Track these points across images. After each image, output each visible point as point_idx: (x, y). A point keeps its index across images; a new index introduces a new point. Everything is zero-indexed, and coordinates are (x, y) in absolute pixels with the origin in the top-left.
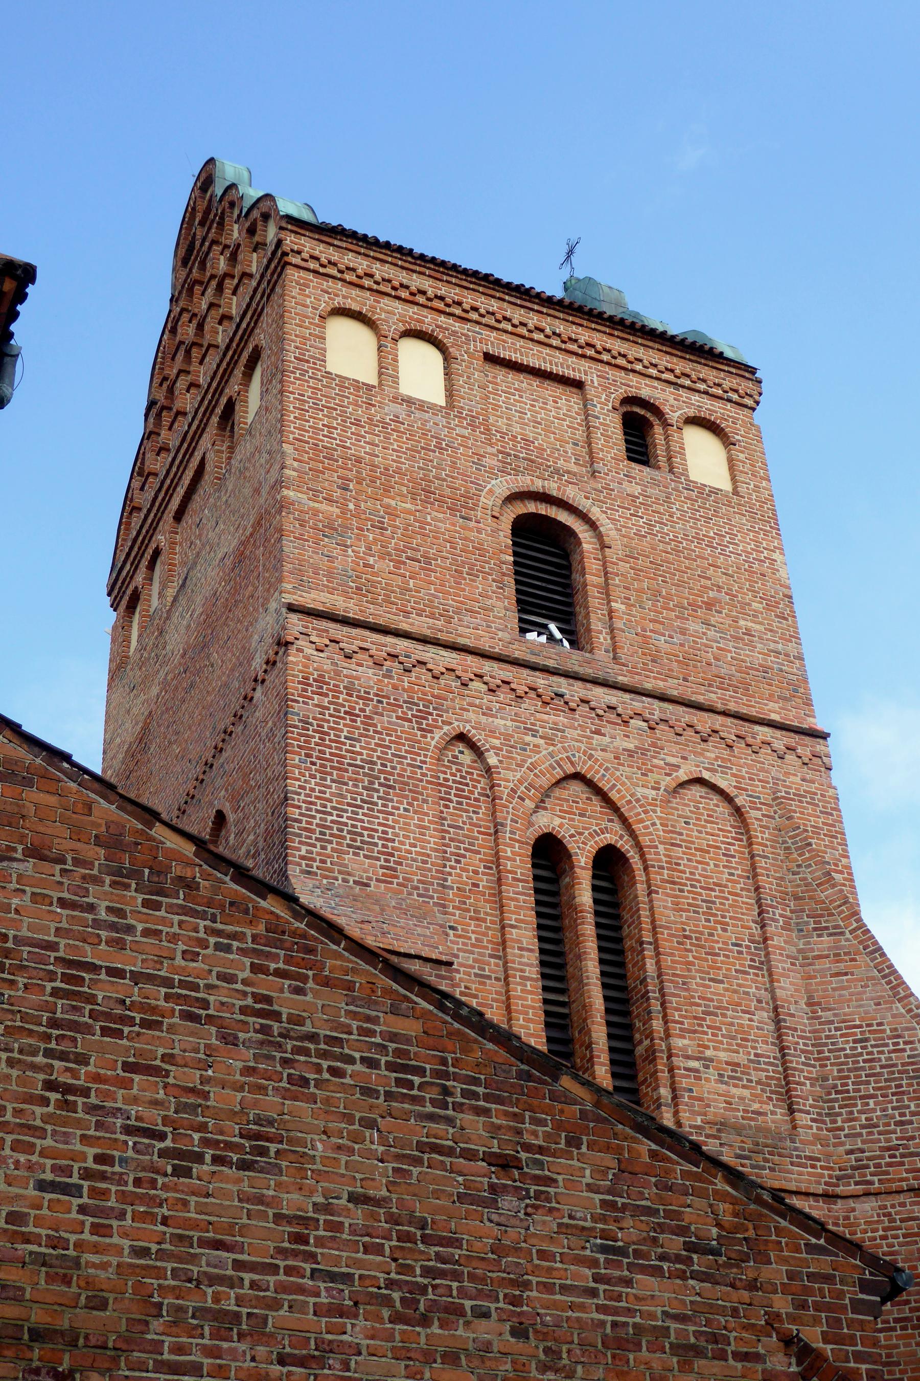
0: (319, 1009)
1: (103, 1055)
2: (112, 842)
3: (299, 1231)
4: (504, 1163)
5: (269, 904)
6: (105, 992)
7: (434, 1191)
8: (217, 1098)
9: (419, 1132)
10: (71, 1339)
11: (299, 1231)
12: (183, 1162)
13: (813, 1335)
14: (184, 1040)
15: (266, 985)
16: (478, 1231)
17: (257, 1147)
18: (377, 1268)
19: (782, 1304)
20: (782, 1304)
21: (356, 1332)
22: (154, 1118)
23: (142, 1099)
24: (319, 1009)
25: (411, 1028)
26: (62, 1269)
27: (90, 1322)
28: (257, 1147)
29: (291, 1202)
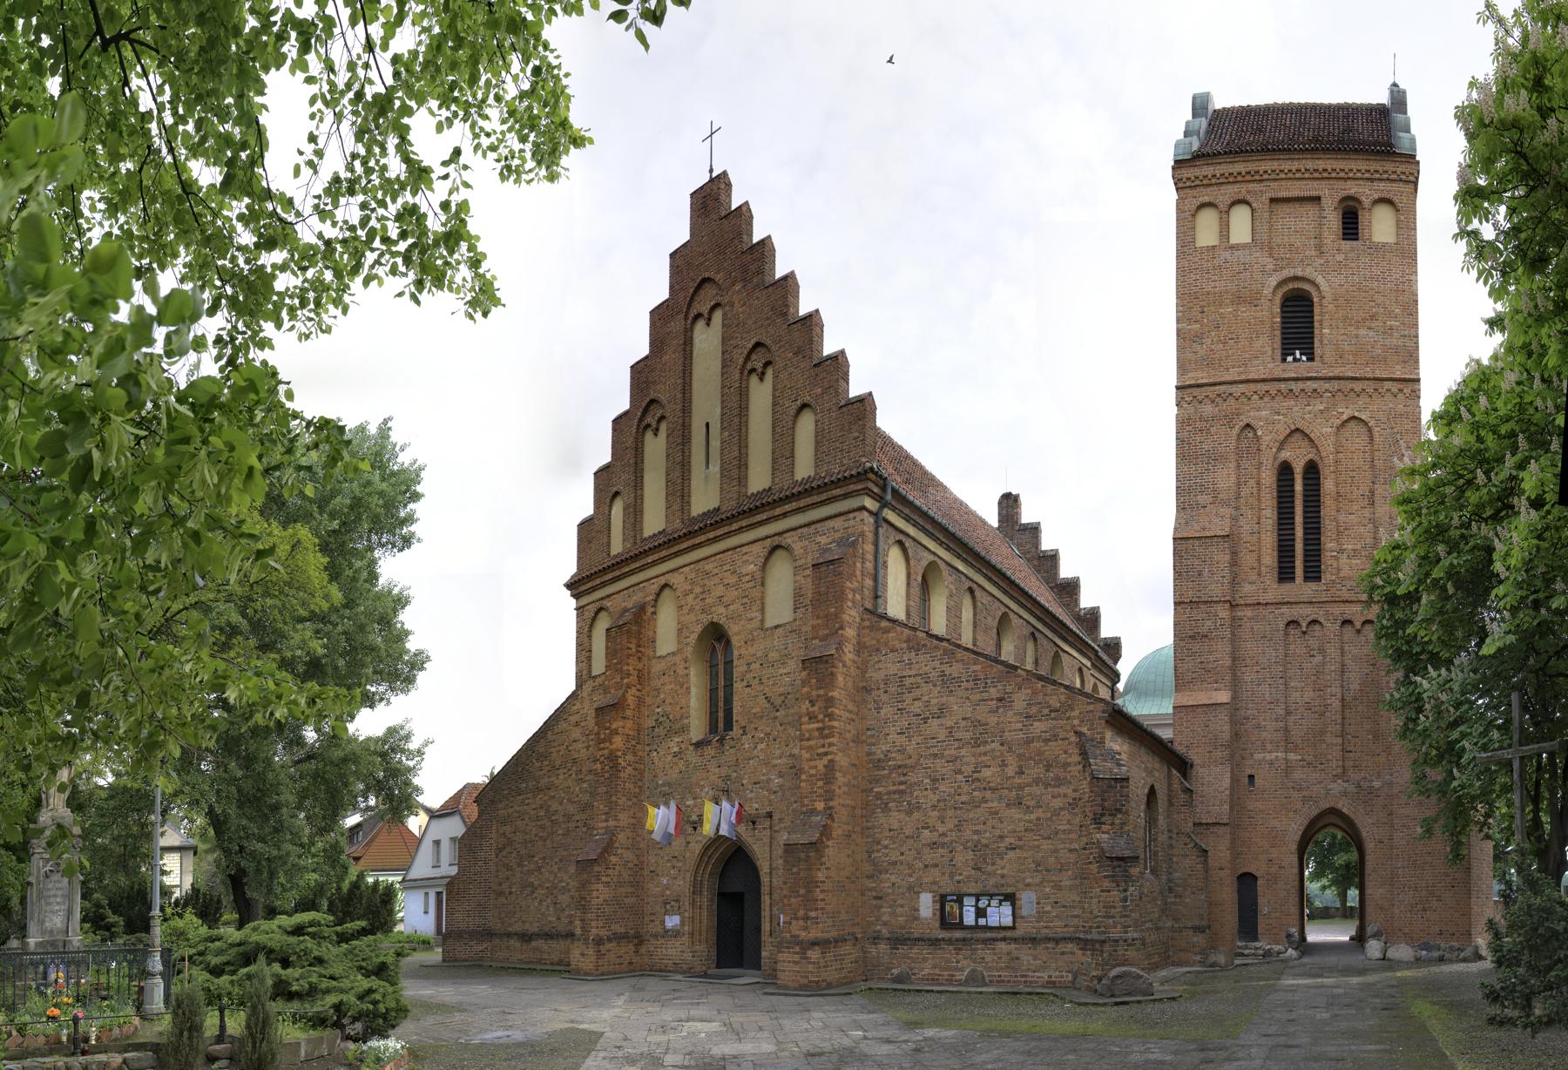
0: (955, 670)
1: (908, 698)
2: (908, 641)
3: (950, 730)
4: (1000, 700)
5: (945, 644)
6: (908, 682)
7: (982, 713)
8: (934, 701)
9: (978, 697)
10: (906, 766)
11: (950, 730)
12: (925, 720)
13: (1084, 730)
14: (925, 688)
15: (944, 667)
16: (993, 720)
17: (942, 711)
18: (968, 735)
19: (1076, 722)
20: (1076, 722)
21: (963, 752)
22: (918, 711)
23: (917, 707)
24: (955, 670)
25: (978, 667)
26: (902, 751)
27: (908, 762)
28: (942, 711)
29: (949, 723)
